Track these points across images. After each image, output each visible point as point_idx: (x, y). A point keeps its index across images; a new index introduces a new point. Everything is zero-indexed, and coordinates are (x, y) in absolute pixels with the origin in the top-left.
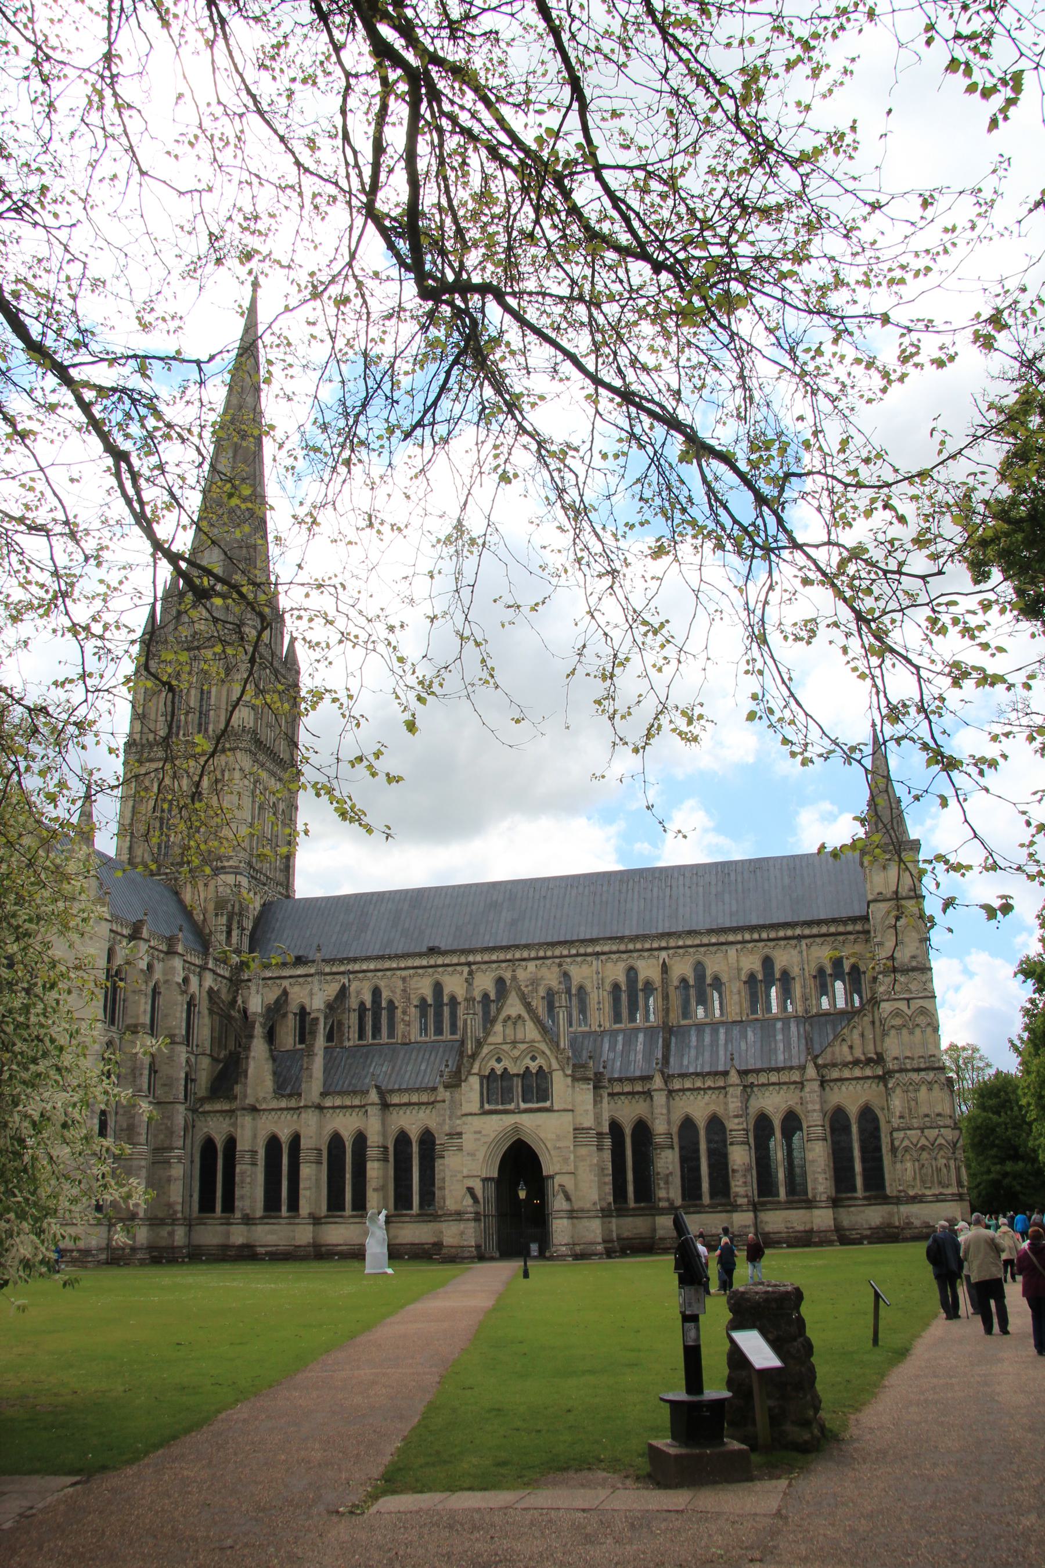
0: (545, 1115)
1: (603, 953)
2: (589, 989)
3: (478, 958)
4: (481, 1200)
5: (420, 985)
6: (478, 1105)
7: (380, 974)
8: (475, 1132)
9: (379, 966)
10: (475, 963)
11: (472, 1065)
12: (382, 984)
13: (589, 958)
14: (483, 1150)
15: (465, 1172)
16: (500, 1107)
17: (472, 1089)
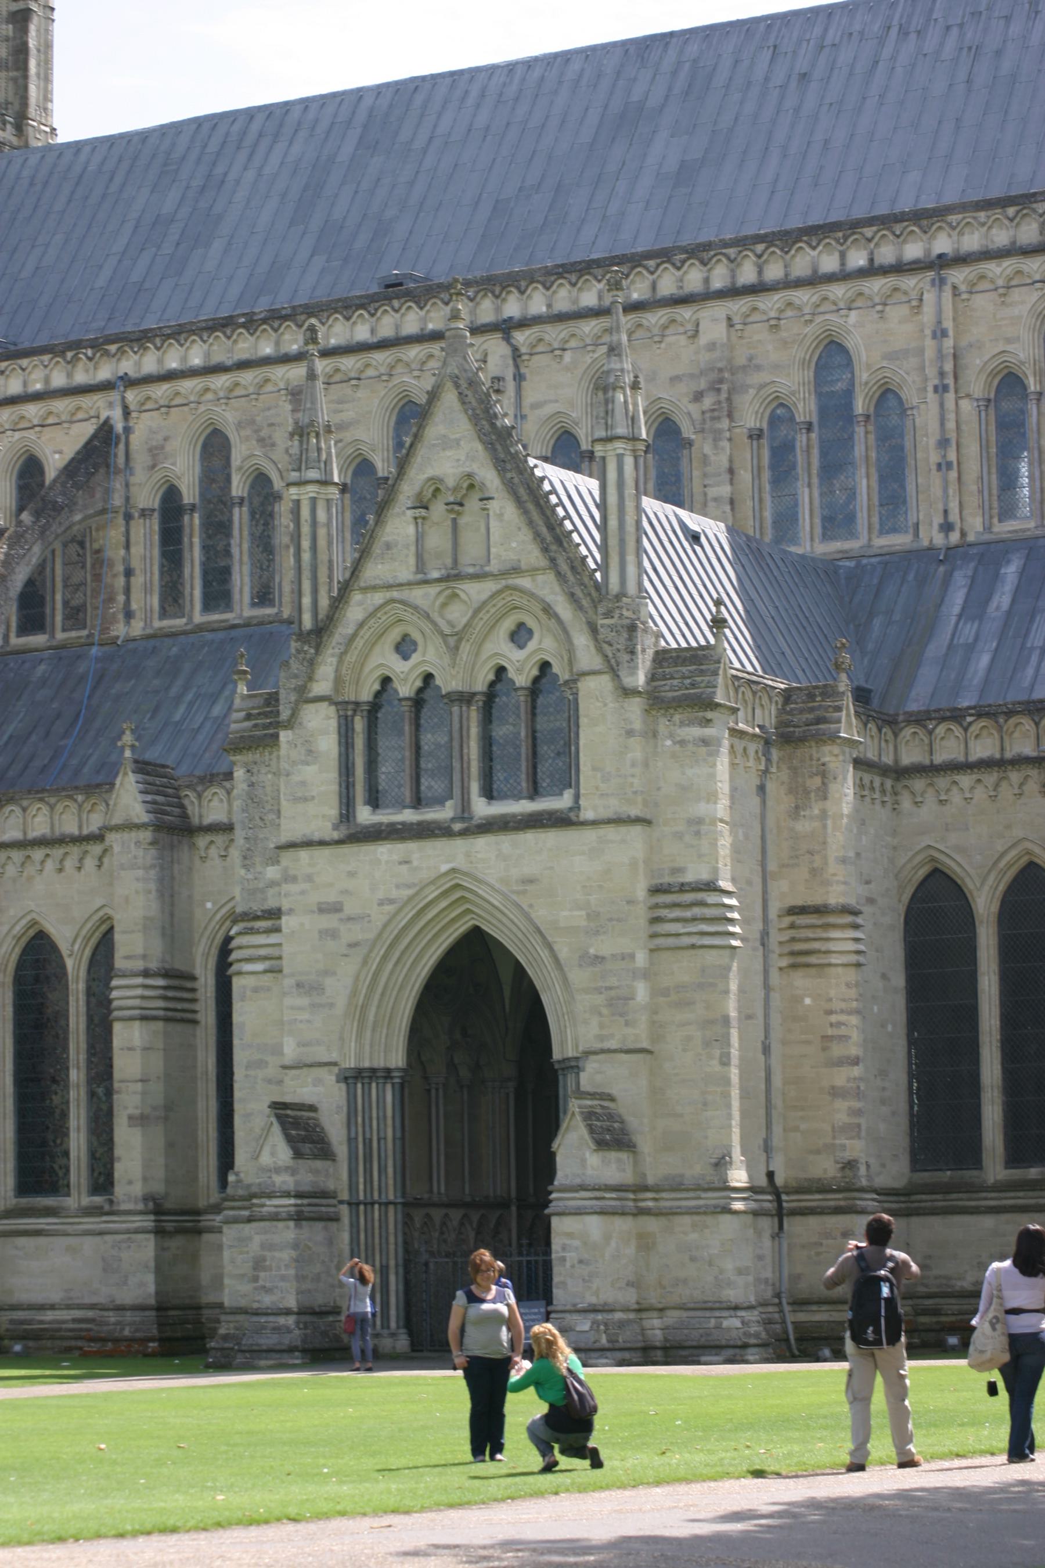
0: (550, 838)
1: (961, 260)
2: (910, 395)
3: (538, 304)
4: (341, 1150)
5: (348, 414)
6: (332, 810)
7: (220, 381)
8: (324, 909)
9: (219, 356)
10: (524, 323)
11: (312, 663)
12: (228, 418)
13: (909, 282)
14: (348, 969)
15: (290, 1050)
16: (409, 816)
17: (312, 755)
